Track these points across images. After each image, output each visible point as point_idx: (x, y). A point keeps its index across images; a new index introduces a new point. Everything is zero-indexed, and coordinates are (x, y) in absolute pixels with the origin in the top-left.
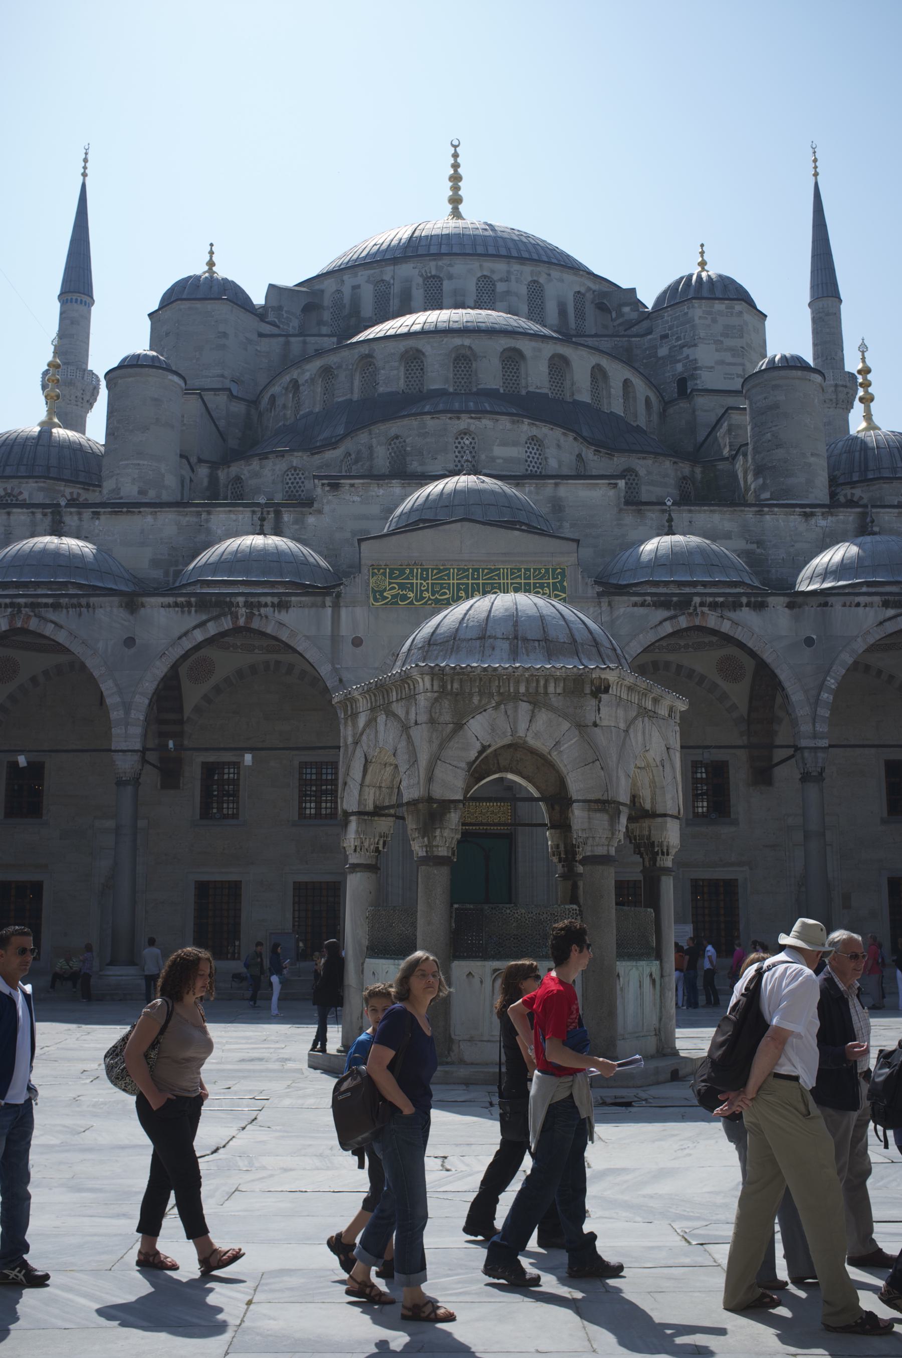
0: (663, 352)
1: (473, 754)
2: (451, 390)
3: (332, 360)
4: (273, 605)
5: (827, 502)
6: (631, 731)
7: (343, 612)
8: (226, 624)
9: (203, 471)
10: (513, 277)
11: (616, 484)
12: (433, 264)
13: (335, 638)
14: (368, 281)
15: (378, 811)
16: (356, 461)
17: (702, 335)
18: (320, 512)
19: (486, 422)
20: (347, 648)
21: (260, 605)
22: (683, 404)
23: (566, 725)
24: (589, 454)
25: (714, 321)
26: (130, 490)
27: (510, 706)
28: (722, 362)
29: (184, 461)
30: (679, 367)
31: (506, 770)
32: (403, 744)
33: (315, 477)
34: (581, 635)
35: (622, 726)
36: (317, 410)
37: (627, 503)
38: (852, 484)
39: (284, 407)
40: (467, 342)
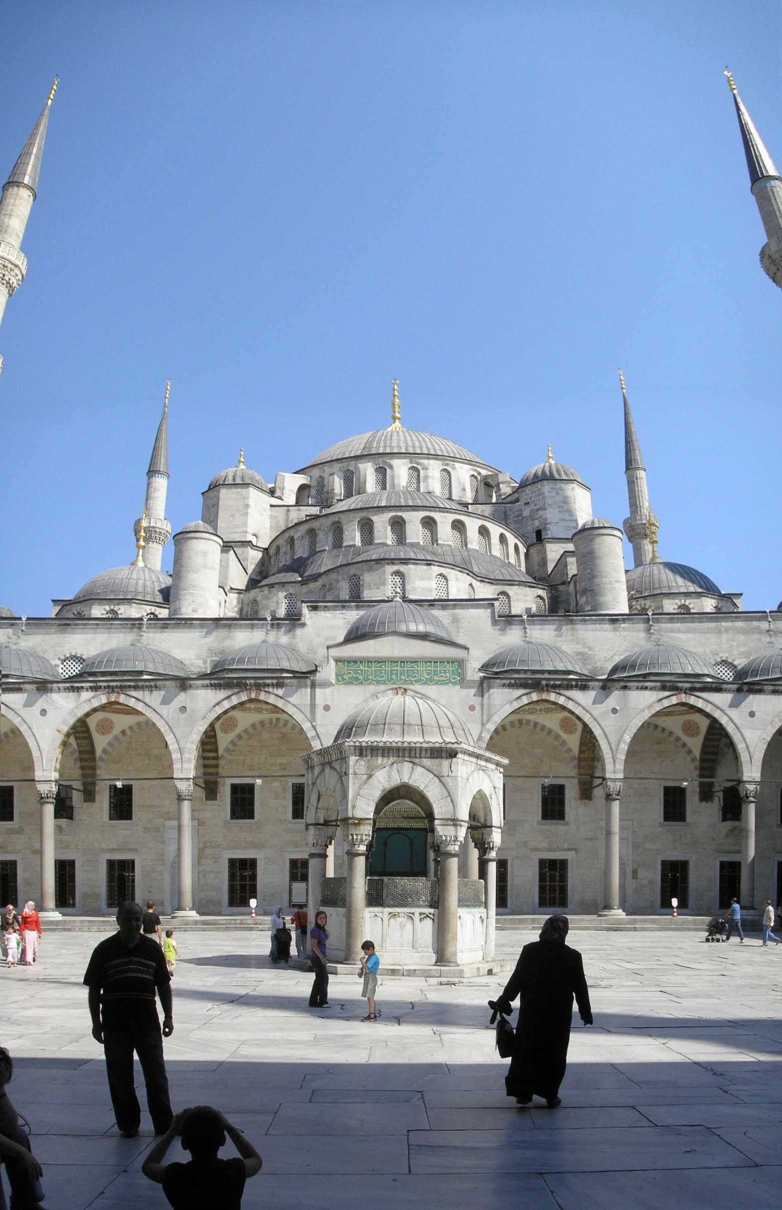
0: (526, 513)
1: (377, 794)
2: (389, 542)
3: (315, 524)
4: (273, 685)
5: (627, 612)
6: (470, 779)
7: (317, 690)
8: (244, 697)
9: (233, 597)
10: (431, 468)
11: (493, 604)
12: (380, 460)
13: (313, 706)
14: (340, 470)
15: (326, 823)
16: (329, 590)
17: (550, 502)
18: (304, 625)
19: (411, 566)
20: (319, 711)
21: (266, 685)
22: (539, 547)
23: (431, 776)
24: (476, 583)
25: (557, 493)
26: (187, 611)
27: (399, 765)
28: (564, 520)
29: (221, 590)
30: (537, 523)
31: (403, 798)
32: (339, 785)
33: (303, 602)
34: (444, 722)
35: (465, 776)
36: (305, 555)
37: (499, 616)
38: (645, 598)
39: (285, 553)
40: (399, 514)
